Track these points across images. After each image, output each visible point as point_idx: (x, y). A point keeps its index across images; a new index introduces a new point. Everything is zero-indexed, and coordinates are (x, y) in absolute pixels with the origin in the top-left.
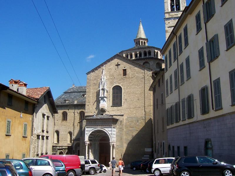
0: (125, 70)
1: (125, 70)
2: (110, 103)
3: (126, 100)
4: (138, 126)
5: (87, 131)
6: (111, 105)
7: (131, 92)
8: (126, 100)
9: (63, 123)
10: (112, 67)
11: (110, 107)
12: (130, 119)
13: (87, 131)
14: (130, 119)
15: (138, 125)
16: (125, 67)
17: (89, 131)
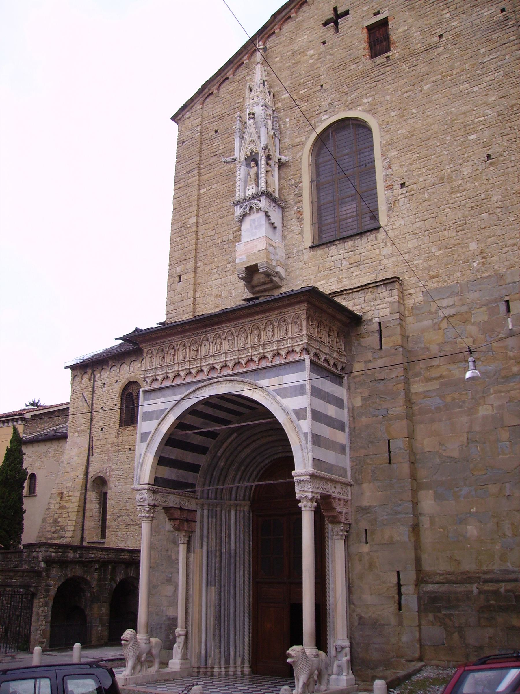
0: (384, 23)
1: (384, 23)
2: (301, 233)
3: (403, 185)
4: (510, 342)
5: (148, 416)
6: (309, 243)
7: (435, 128)
8: (403, 185)
9: (125, 438)
10: (303, 39)
11: (307, 255)
12: (445, 303)
13: (148, 416)
14: (445, 303)
15: (512, 334)
16: (378, 13)
17: (162, 415)
